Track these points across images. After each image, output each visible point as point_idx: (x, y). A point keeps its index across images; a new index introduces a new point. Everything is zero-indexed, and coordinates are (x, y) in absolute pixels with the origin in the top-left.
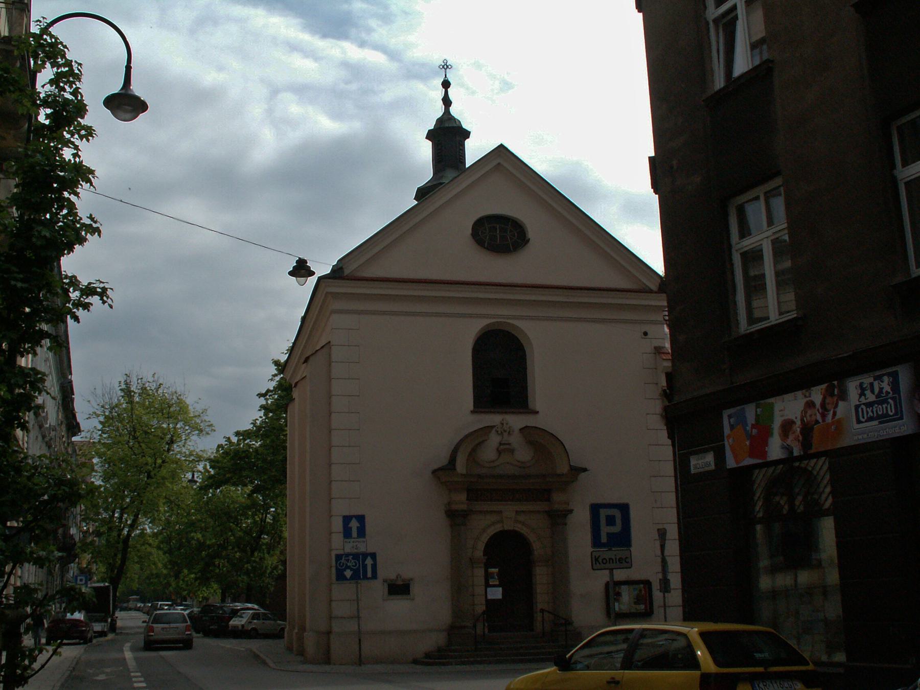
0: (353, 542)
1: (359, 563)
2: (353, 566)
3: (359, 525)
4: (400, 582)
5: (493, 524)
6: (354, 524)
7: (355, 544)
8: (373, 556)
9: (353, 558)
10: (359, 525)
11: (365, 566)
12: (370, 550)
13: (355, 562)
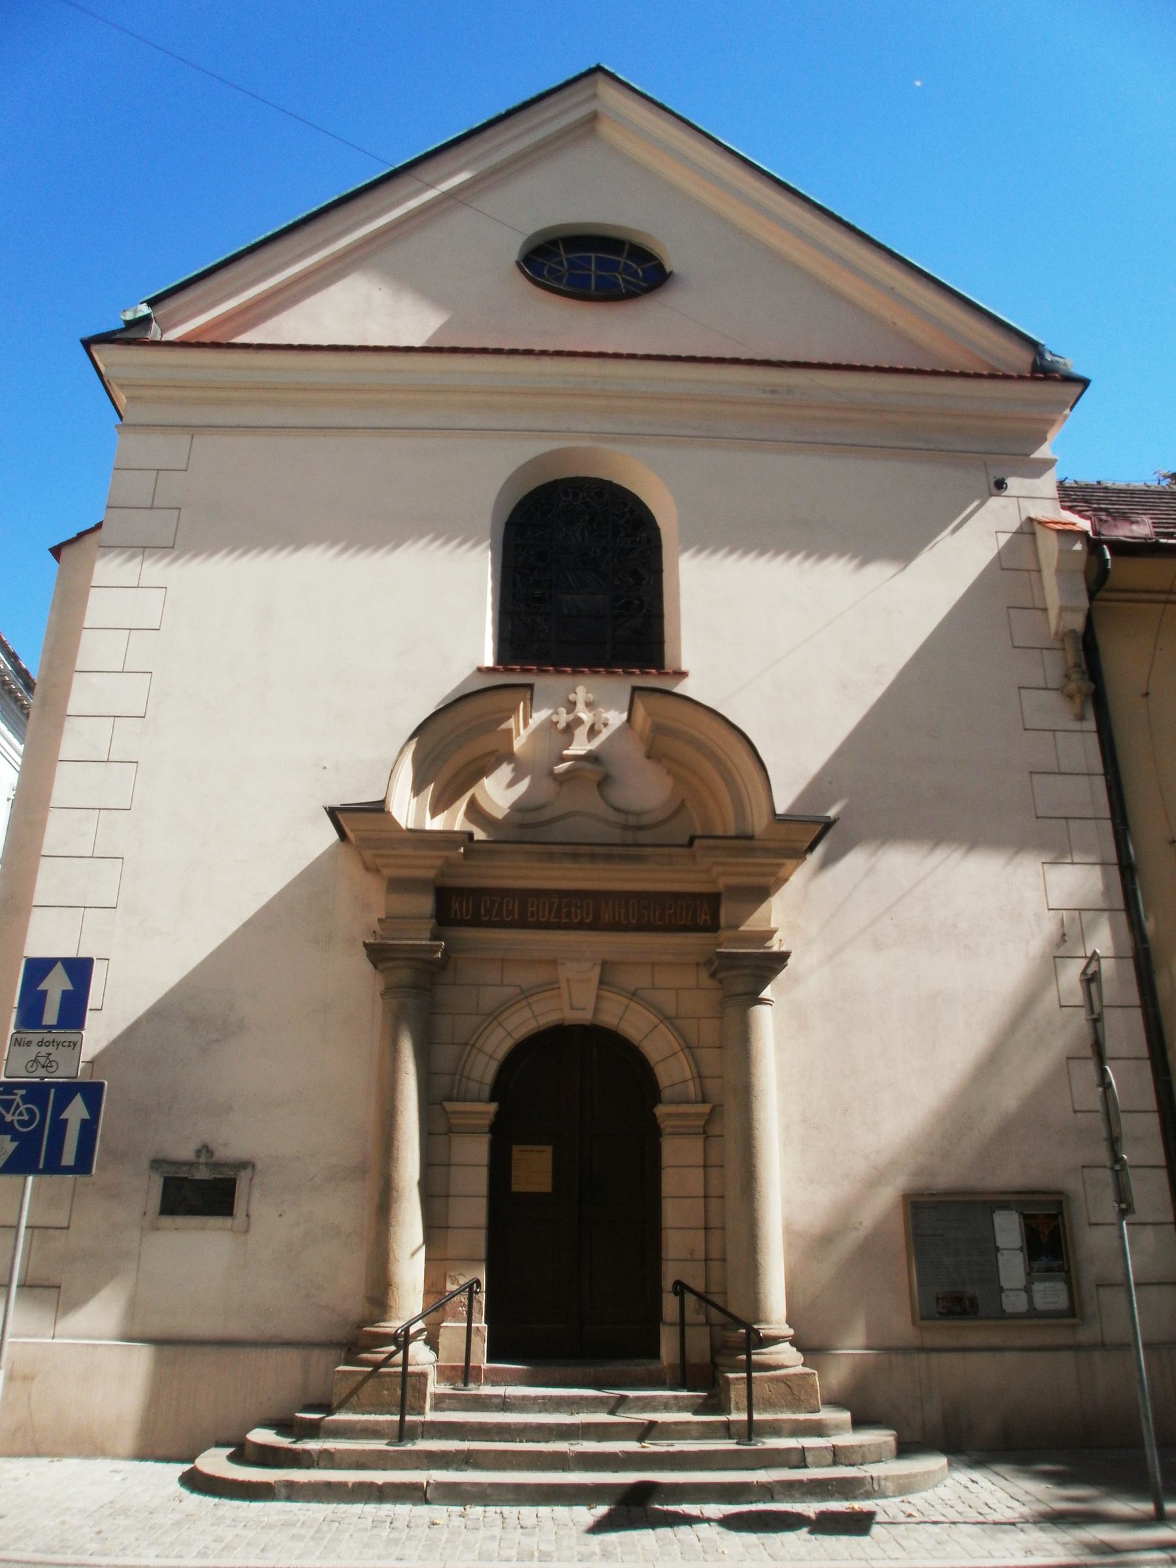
0: (41, 1043)
1: (43, 1118)
2: (23, 1123)
3: (69, 987)
4: (203, 1174)
5: (526, 994)
6: (56, 985)
7: (44, 1050)
8: (92, 1093)
9: (25, 1099)
10: (69, 987)
11: (60, 1127)
12: (82, 1076)
13: (29, 1111)
